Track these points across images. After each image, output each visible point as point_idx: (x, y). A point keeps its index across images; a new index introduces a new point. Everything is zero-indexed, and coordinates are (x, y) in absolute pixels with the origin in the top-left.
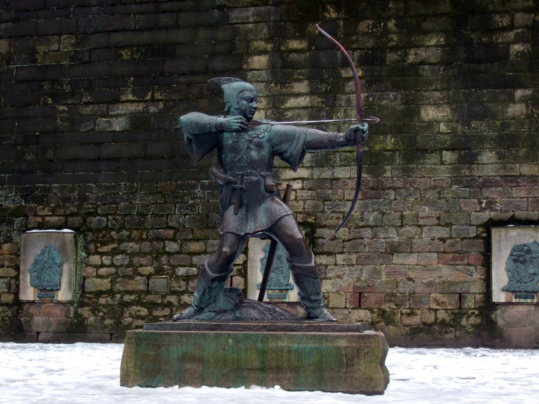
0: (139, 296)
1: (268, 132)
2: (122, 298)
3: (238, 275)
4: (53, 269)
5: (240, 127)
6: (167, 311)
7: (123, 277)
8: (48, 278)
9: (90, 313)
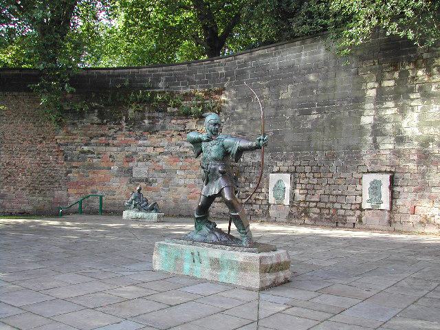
6: (327, 211)
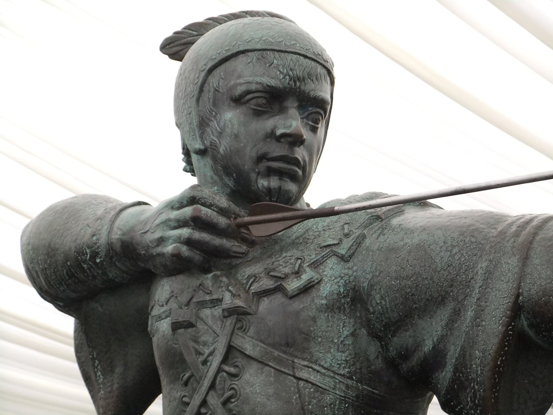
1: (343, 259)
5: (189, 242)
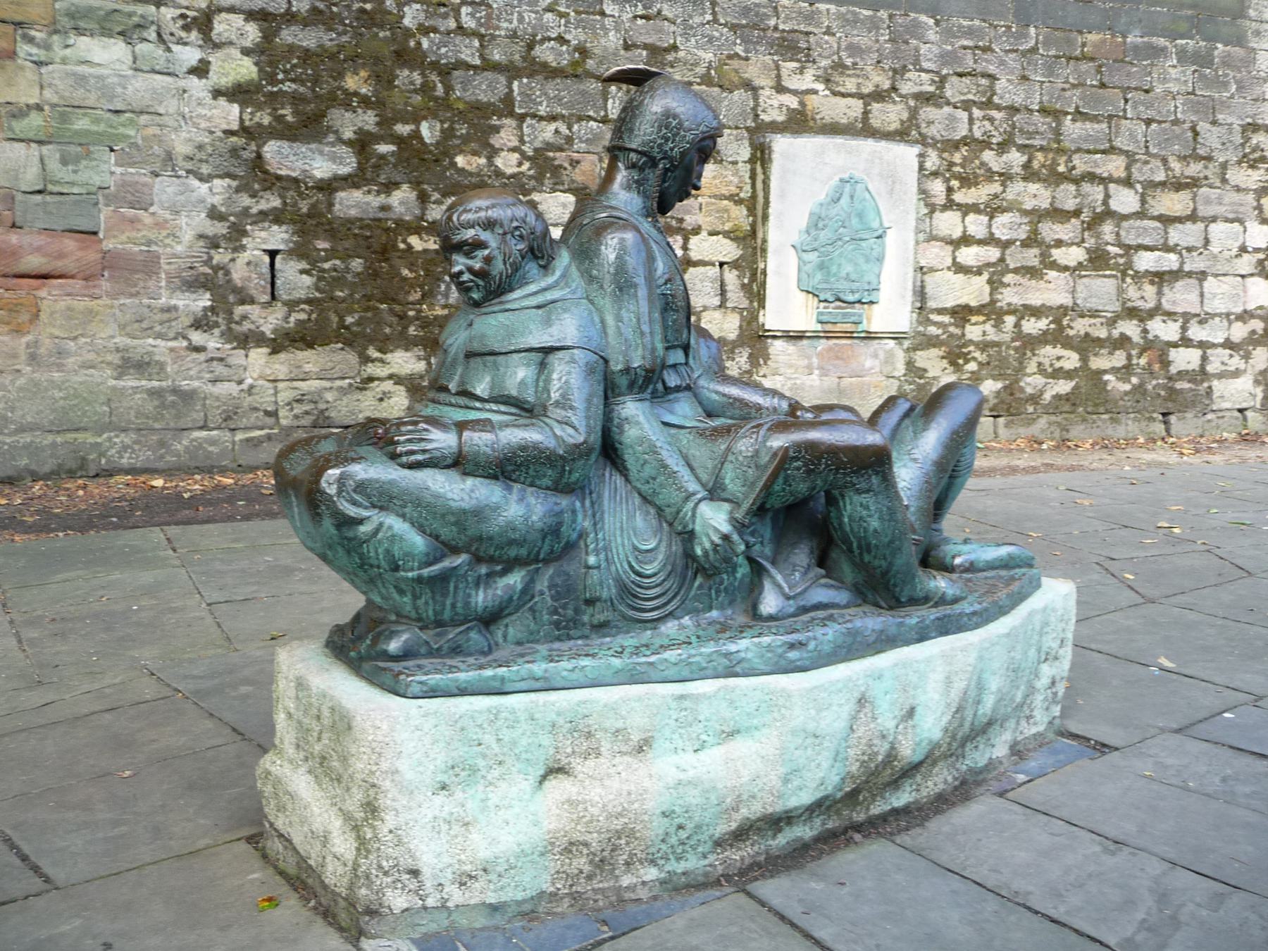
0: (1057, 321)
2: (1017, 325)
3: (1259, 275)
4: (864, 244)
6: (1119, 359)
7: (1016, 271)
8: (848, 268)
9: (945, 363)
